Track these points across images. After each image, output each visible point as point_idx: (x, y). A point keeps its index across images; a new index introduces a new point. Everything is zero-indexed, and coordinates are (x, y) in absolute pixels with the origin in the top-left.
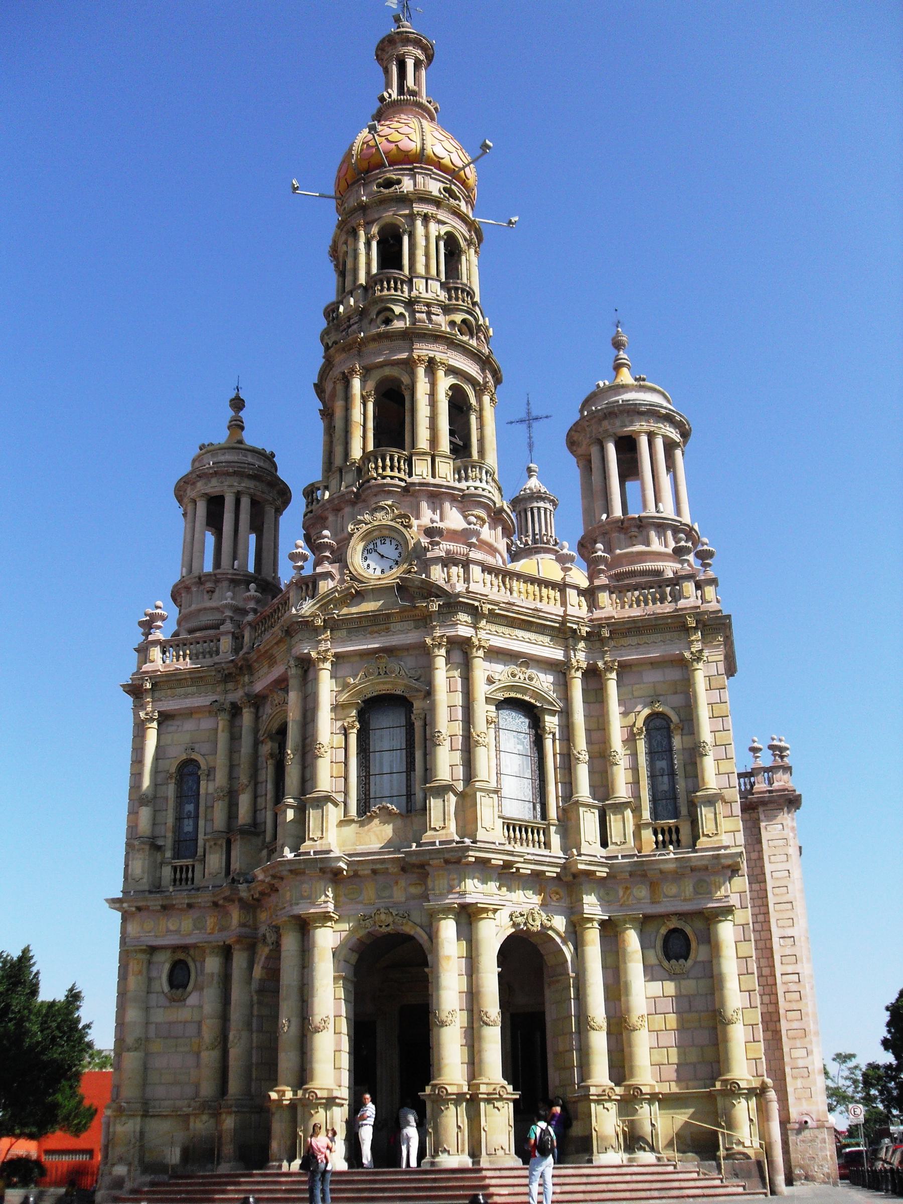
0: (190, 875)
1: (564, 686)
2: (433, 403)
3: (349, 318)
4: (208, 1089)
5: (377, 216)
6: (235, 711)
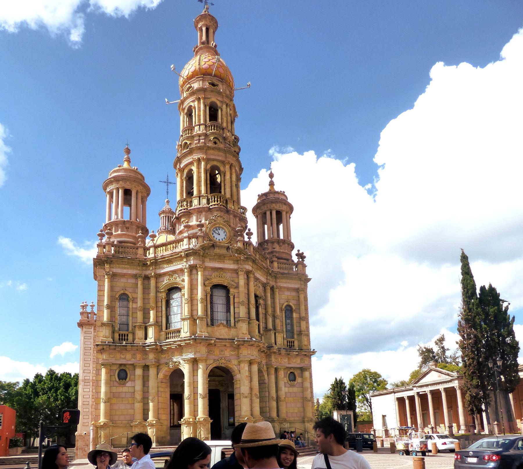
0: (126, 338)
5: (209, 97)
6: (147, 278)
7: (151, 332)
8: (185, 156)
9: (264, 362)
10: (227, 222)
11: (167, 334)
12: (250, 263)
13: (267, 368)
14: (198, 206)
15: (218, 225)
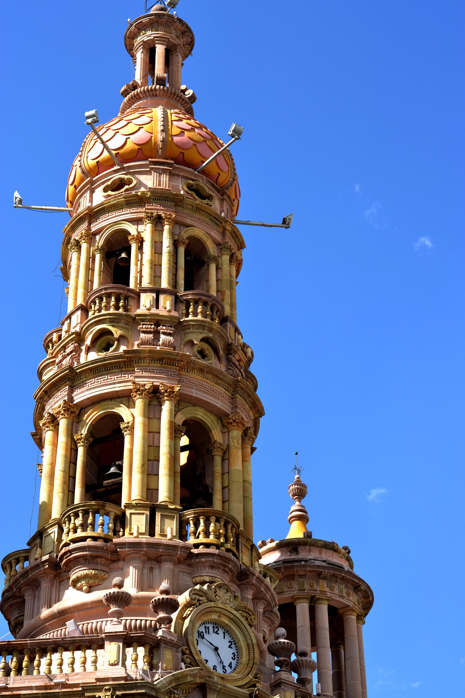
3: (157, 324)
5: (189, 222)
8: (98, 370)
14: (145, 539)
15: (214, 617)
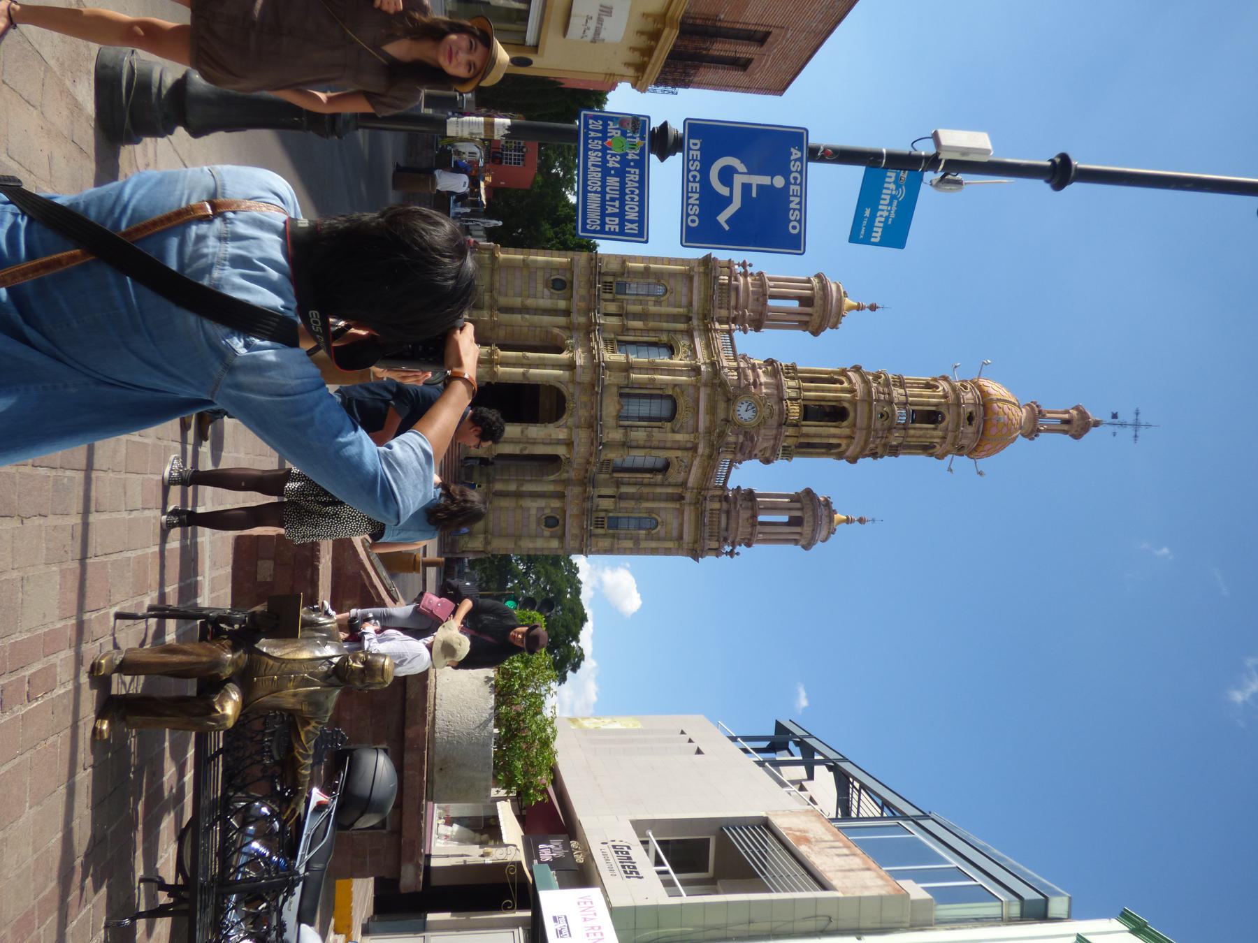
1: (676, 485)
2: (829, 436)
4: (503, 301)
7: (614, 321)
9: (573, 475)
10: (762, 423)
11: (611, 341)
12: (707, 451)
13: (563, 481)
